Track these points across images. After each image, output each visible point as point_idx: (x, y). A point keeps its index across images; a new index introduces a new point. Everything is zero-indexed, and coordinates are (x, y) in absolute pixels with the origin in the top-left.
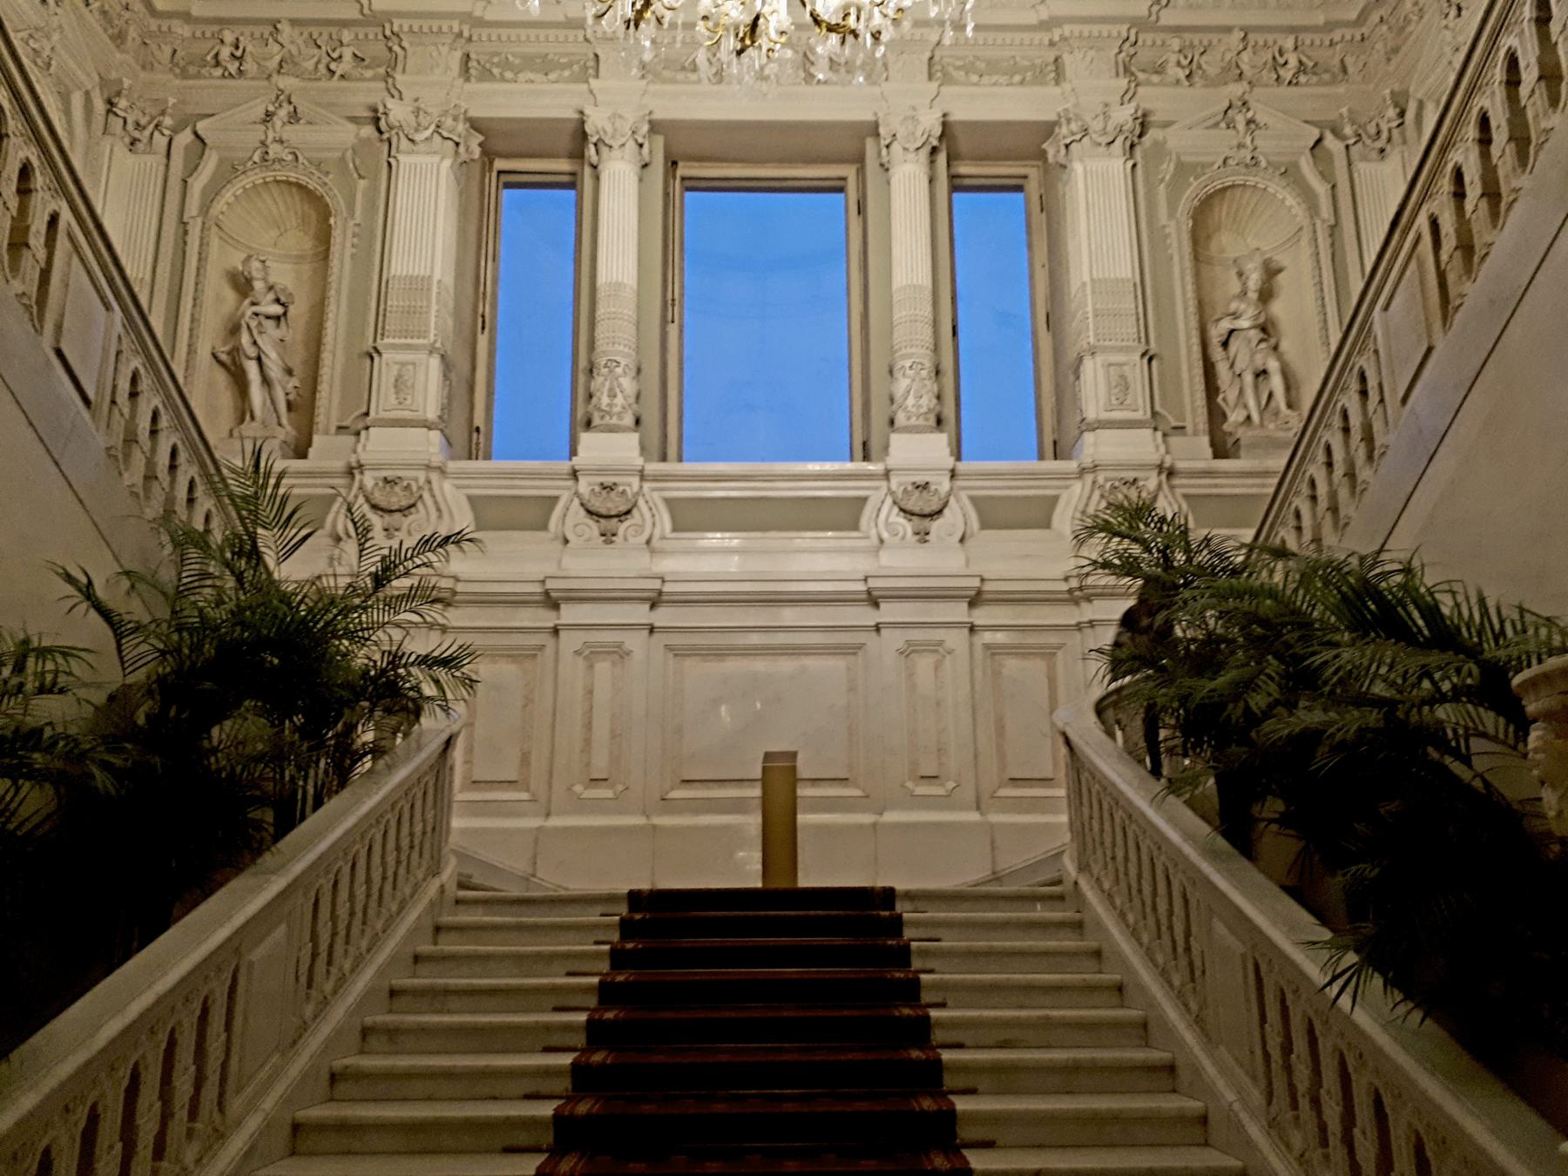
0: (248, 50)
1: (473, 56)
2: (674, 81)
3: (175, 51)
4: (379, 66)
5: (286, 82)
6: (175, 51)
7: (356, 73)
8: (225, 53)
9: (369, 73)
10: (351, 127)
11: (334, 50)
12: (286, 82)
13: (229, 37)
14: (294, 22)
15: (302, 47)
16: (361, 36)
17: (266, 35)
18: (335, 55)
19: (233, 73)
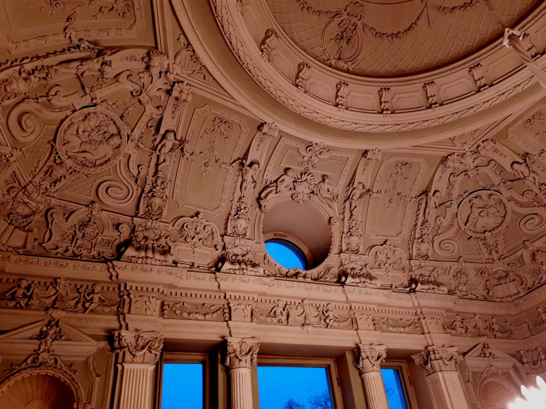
0: (35, 291)
1: (166, 303)
2: (266, 323)
4: (113, 305)
5: (57, 314)
7: (99, 309)
8: (20, 292)
9: (107, 310)
10: (94, 342)
11: (88, 295)
12: (57, 314)
13: (24, 284)
14: (67, 279)
15: (69, 292)
16: (105, 289)
17: (48, 284)
18: (88, 298)
19: (23, 305)
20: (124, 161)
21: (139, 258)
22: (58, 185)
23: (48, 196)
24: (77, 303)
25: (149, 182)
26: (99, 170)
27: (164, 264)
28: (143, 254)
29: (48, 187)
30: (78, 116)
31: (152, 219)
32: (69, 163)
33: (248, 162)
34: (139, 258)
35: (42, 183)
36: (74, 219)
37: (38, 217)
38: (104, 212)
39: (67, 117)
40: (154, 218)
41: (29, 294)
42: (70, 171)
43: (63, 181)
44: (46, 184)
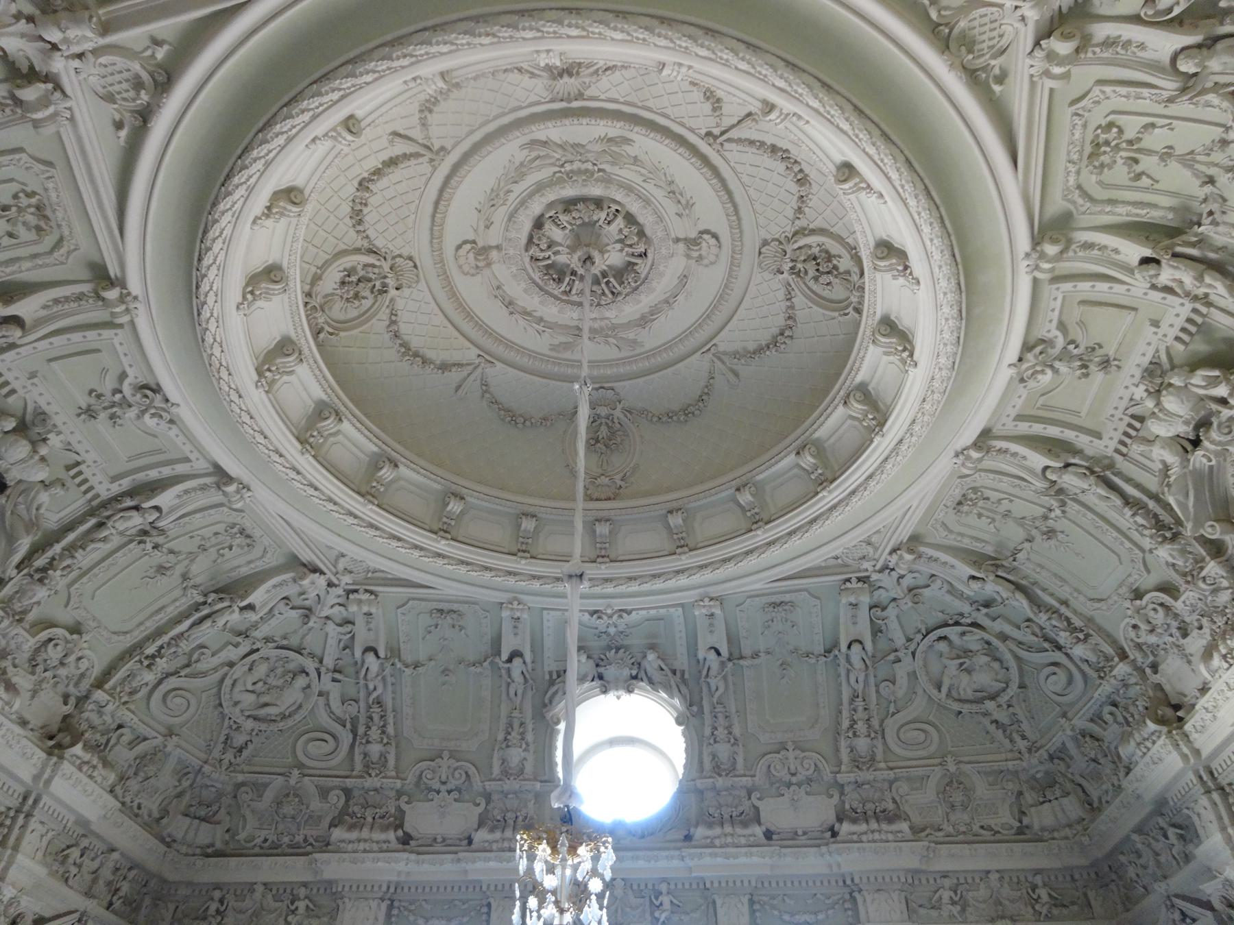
3: (177, 907)
6: (177, 907)
13: (217, 894)
20: (322, 700)
21: (350, 842)
22: (245, 753)
23: (233, 771)
24: (280, 915)
25: (362, 720)
26: (290, 722)
27: (385, 846)
28: (354, 835)
29: (233, 760)
30: (238, 671)
31: (370, 776)
32: (249, 724)
33: (505, 656)
34: (350, 842)
35: (223, 757)
36: (269, 795)
37: (226, 801)
38: (307, 778)
39: (226, 675)
40: (373, 774)
41: (222, 909)
42: (254, 733)
43: (250, 747)
44: (229, 756)
